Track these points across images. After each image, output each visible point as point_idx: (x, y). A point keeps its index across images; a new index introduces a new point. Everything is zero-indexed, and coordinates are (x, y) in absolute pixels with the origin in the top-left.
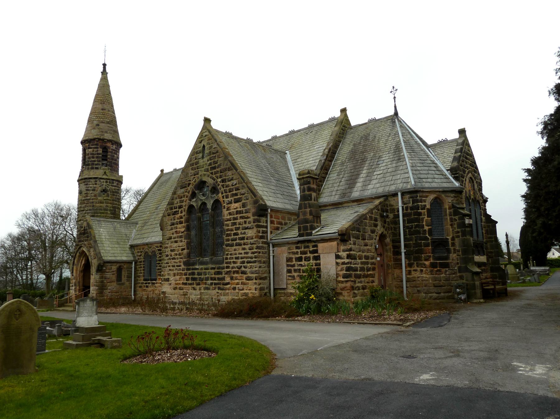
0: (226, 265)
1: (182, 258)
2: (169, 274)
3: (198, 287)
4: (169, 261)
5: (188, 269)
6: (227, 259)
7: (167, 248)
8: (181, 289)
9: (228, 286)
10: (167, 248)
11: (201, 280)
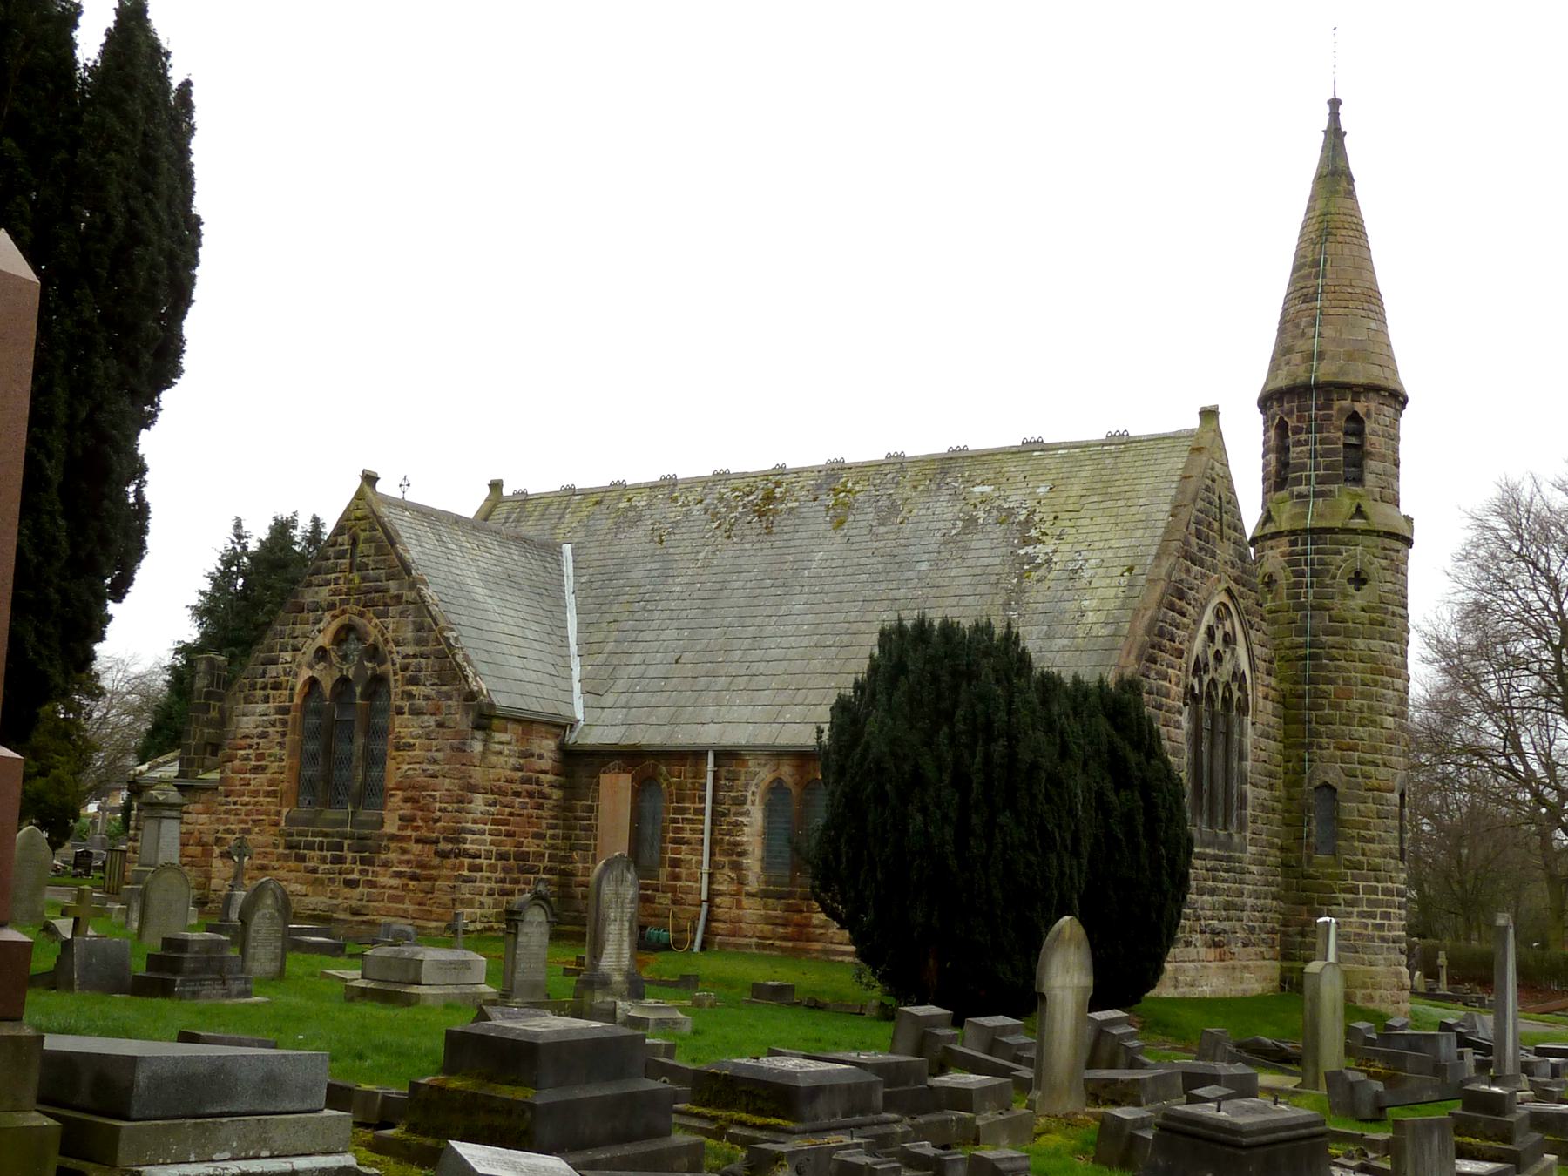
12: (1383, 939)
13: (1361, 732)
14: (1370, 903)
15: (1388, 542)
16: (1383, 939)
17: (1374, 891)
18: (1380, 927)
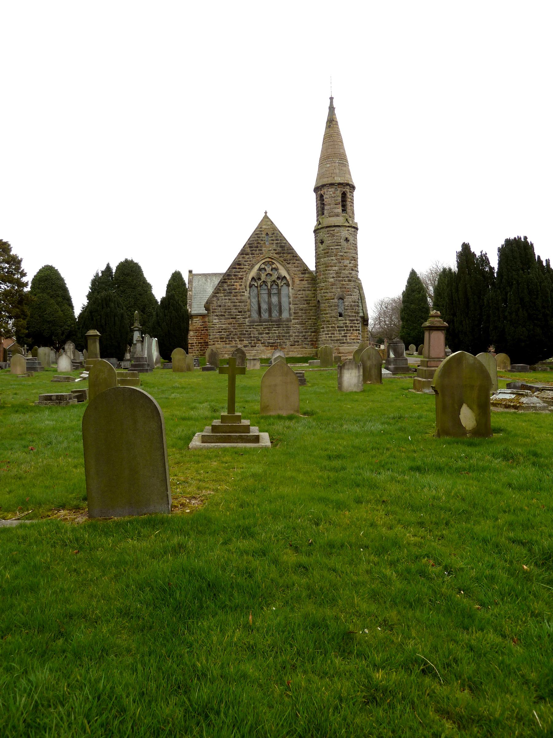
12: (332, 340)
13: (323, 284)
14: (328, 331)
15: (328, 229)
16: (332, 340)
17: (328, 327)
18: (331, 337)
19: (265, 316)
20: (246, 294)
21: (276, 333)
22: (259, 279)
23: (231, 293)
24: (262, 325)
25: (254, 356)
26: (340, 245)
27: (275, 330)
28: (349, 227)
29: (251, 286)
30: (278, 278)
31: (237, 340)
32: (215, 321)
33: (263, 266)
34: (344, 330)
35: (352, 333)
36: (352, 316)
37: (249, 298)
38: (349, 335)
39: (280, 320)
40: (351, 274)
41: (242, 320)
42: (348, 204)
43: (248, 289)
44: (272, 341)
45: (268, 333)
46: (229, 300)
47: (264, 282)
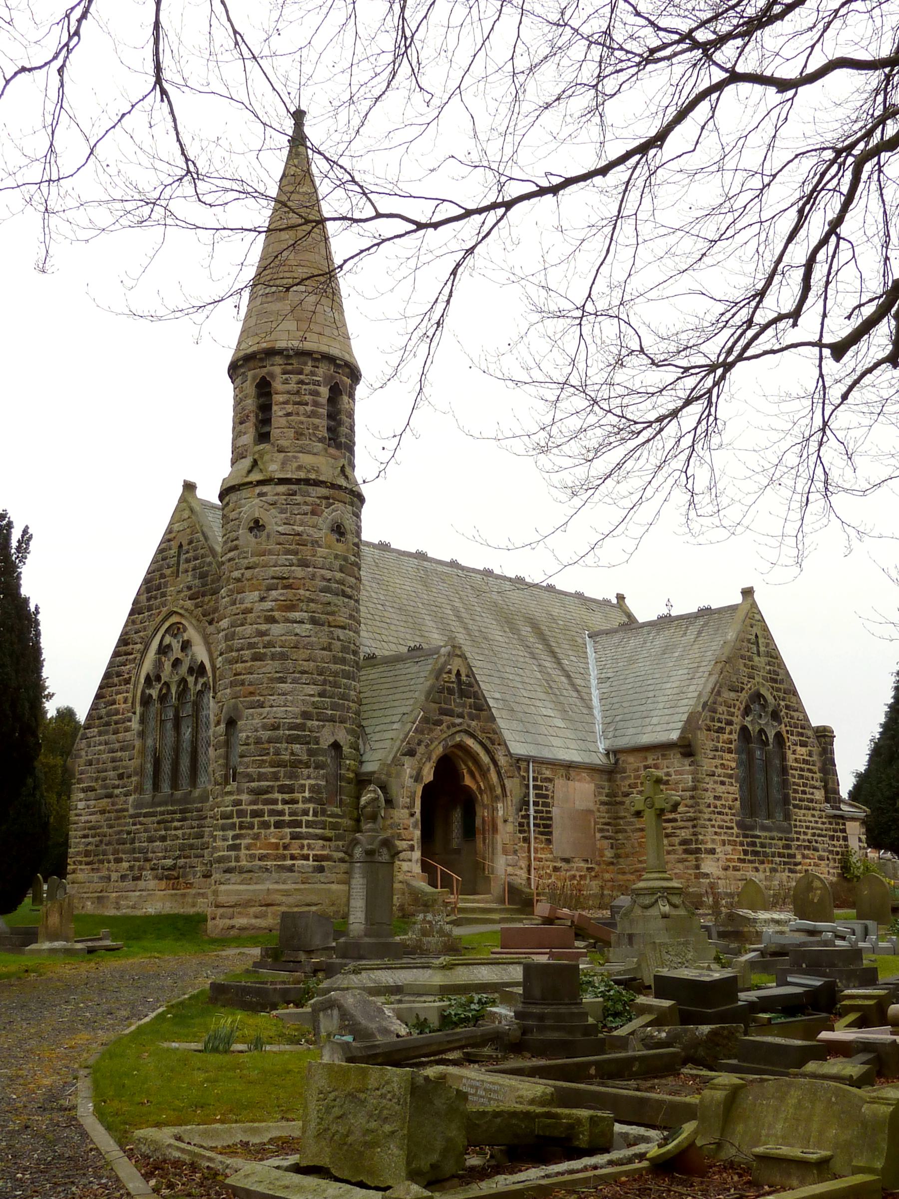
0: (795, 836)
1: (733, 815)
2: (713, 841)
3: (763, 866)
4: (713, 816)
5: (745, 836)
6: (796, 826)
7: (706, 790)
8: (736, 869)
9: (799, 867)
10: (706, 790)
11: (765, 854)
19: (166, 788)
20: (135, 725)
21: (178, 838)
22: (158, 678)
23: (108, 724)
24: (153, 814)
25: (133, 907)
26: (236, 548)
27: (176, 829)
28: (260, 483)
29: (146, 701)
30: (191, 671)
31: (111, 857)
32: (81, 805)
33: (168, 640)
34: (233, 827)
35: (257, 837)
36: (261, 777)
37: (142, 734)
38: (248, 841)
39: (187, 799)
40: (262, 634)
41: (123, 798)
42: (250, 404)
43: (138, 709)
44: (169, 862)
45: (163, 839)
46: (106, 744)
47: (165, 683)
